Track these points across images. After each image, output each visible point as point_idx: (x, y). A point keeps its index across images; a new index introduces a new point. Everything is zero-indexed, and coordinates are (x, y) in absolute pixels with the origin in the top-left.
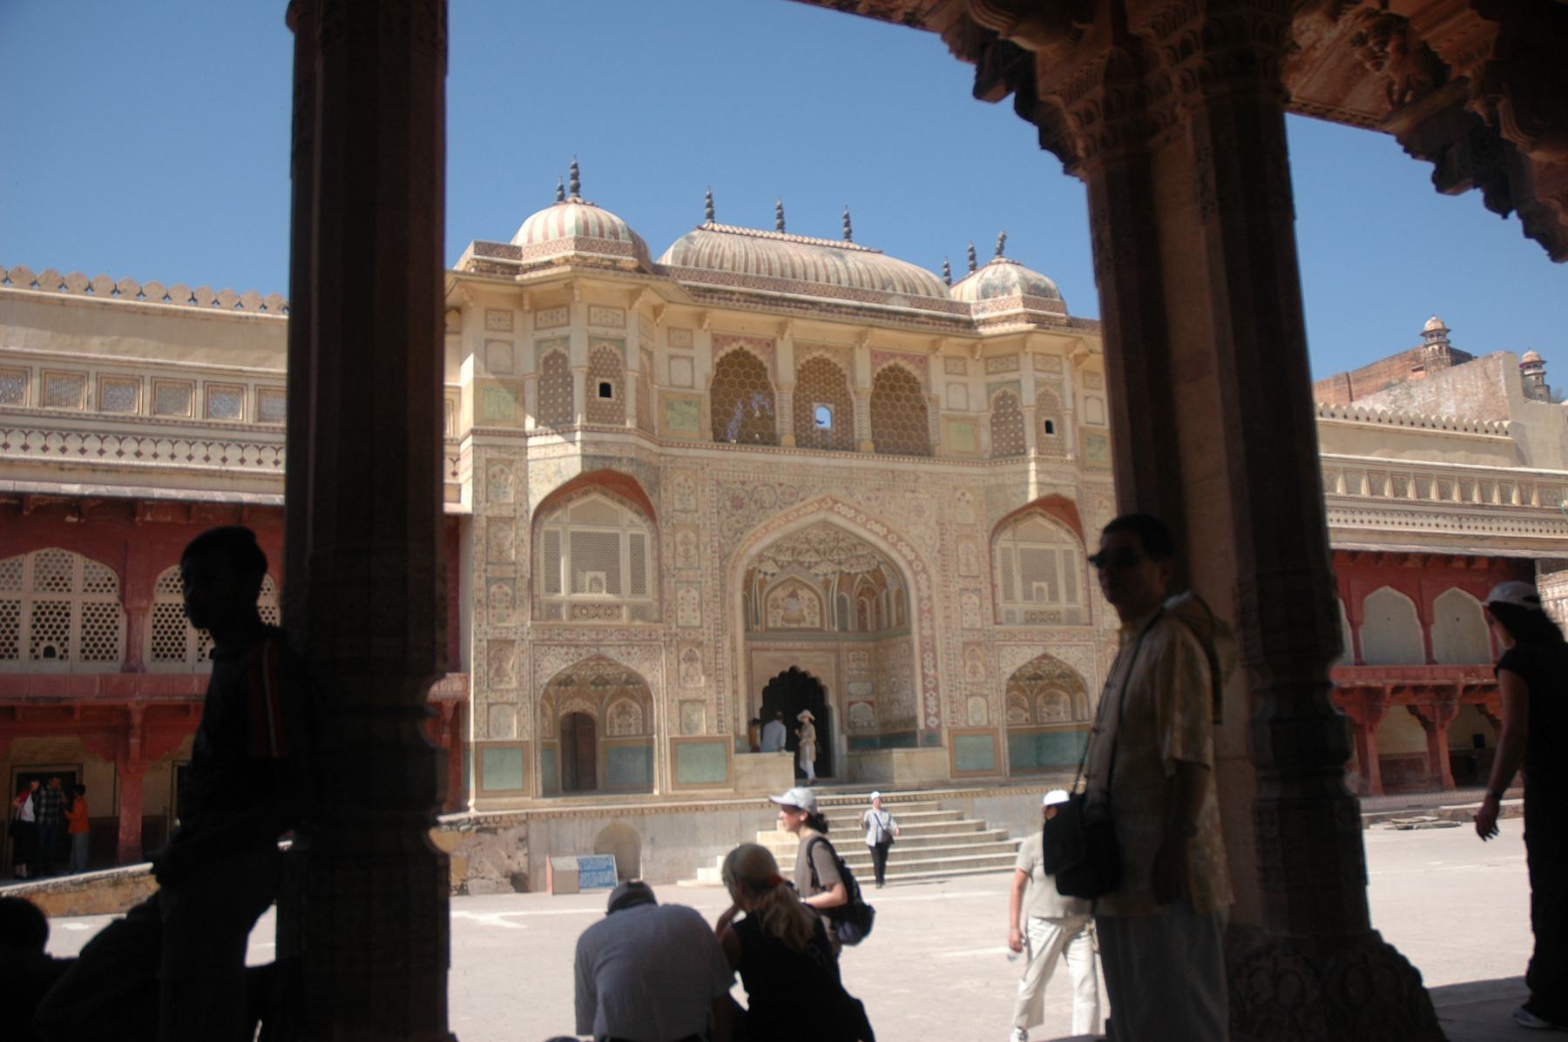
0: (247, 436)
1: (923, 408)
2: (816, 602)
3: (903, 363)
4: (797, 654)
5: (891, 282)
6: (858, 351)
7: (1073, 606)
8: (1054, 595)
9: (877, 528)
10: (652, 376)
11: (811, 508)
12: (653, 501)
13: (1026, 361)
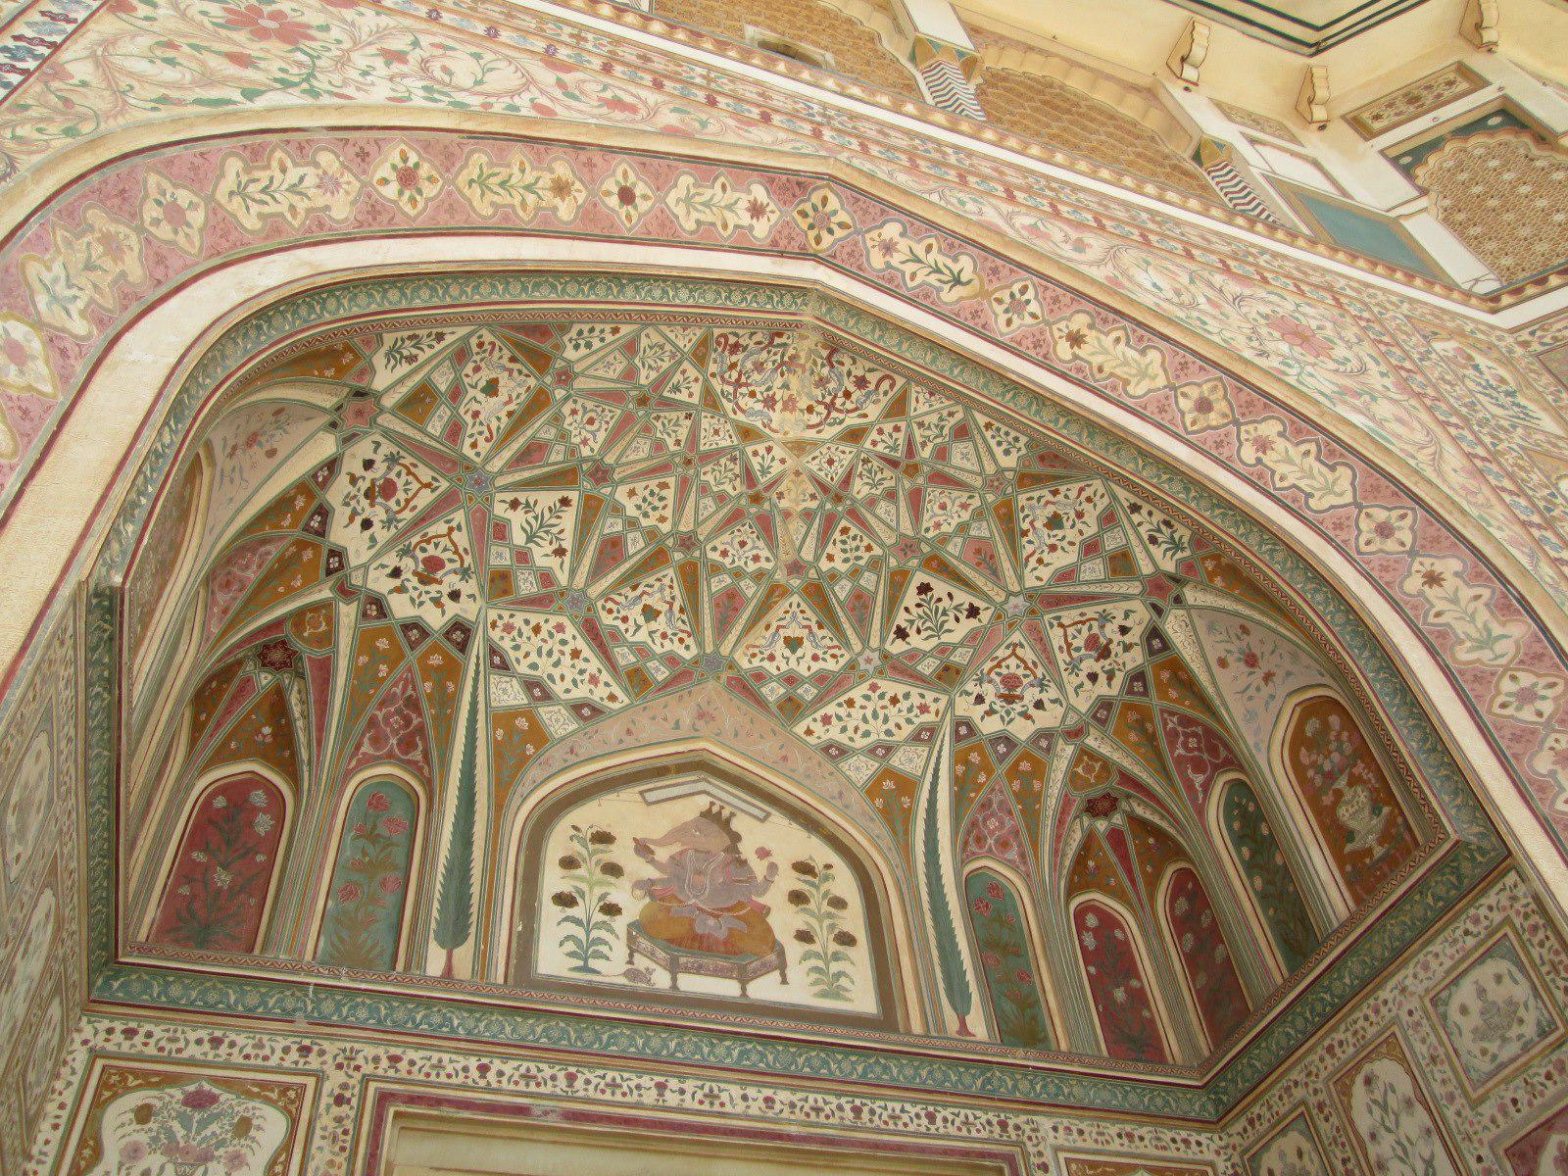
9: (1106, 351)
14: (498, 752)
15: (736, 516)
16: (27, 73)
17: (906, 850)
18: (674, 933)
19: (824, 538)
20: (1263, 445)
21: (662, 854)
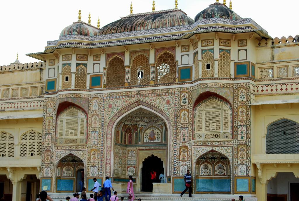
0: (9, 101)
1: (175, 66)
2: (160, 133)
3: (168, 51)
4: (153, 151)
5: (166, 24)
6: (151, 50)
7: (226, 131)
8: (218, 128)
9: (155, 109)
10: (86, 71)
11: (134, 105)
13: (200, 44)
14: (141, 130)
18: (151, 139)
21: (150, 133)
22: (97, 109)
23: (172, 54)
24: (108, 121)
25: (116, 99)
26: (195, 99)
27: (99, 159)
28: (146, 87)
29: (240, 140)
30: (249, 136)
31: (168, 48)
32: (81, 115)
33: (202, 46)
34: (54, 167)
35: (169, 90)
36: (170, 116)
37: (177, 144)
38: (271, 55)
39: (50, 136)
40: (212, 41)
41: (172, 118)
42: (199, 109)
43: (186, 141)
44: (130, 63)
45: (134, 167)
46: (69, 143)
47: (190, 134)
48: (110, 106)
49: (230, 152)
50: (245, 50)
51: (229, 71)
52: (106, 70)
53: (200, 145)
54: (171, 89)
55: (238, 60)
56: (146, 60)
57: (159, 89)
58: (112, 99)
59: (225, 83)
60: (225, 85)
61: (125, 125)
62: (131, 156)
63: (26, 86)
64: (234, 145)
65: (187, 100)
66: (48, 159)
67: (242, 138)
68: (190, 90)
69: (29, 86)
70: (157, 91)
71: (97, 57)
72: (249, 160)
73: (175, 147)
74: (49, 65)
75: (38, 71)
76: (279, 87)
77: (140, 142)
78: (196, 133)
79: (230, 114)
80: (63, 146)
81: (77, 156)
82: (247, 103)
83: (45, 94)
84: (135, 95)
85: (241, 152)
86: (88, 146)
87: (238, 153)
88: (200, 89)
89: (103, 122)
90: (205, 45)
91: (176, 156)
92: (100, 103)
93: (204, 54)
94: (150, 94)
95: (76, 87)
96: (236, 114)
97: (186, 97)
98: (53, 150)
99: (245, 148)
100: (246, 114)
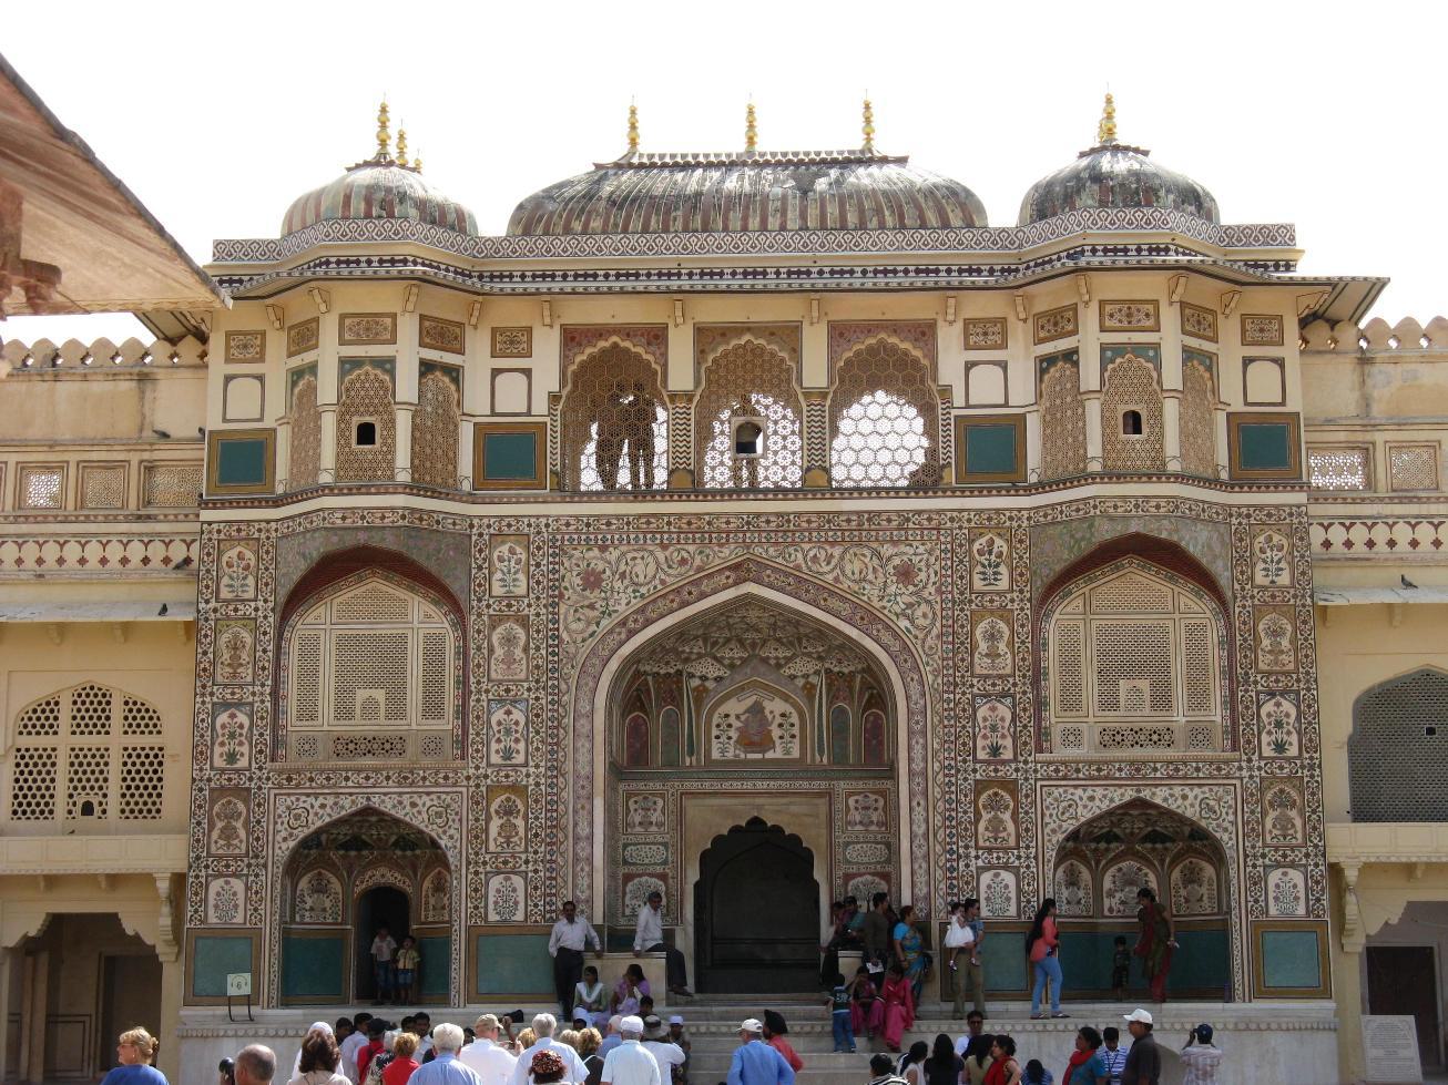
2: (795, 719)
3: (893, 340)
5: (879, 211)
6: (807, 331)
7: (1200, 716)
8: (1162, 700)
9: (834, 603)
12: (455, 587)
13: (1090, 318)
15: (747, 630)
16: (557, 646)
17: (812, 707)
18: (746, 742)
19: (775, 630)
20: (878, 631)
21: (743, 718)
22: (521, 589)
23: (917, 353)
24: (584, 651)
25: (624, 549)
26: (1058, 568)
27: (536, 835)
28: (791, 496)
29: (1273, 759)
30: (1311, 740)
31: (895, 327)
32: (428, 616)
33: (1103, 330)
34: (271, 877)
35: (908, 520)
36: (916, 638)
37: (958, 771)
38: (1356, 394)
39: (242, 718)
40: (1150, 308)
41: (931, 652)
42: (1066, 614)
43: (1003, 757)
44: (697, 383)
45: (663, 877)
46: (354, 753)
47: (1025, 726)
48: (592, 580)
49: (1224, 811)
50: (1274, 360)
51: (1213, 450)
52: (560, 407)
53: (1075, 776)
54: (919, 512)
55: (1247, 404)
56: (776, 372)
57: (859, 513)
58: (603, 549)
59: (1203, 502)
60: (1204, 510)
61: (638, 674)
62: (640, 823)
63: (52, 457)
64: (1241, 779)
65: (1003, 569)
66: (228, 834)
67: (1280, 747)
68: (1015, 524)
69: (73, 458)
70: (849, 521)
71: (512, 342)
72: (1316, 846)
73: (950, 784)
74: (228, 360)
75: (126, 386)
76: (1402, 533)
77: (691, 754)
78: (1053, 720)
79: (1216, 640)
80: (322, 771)
81: (407, 819)
82: (1295, 596)
83: (204, 504)
84: (728, 533)
85: (1277, 813)
86: (472, 771)
87: (1264, 814)
88: (1096, 524)
89: (554, 654)
90: (1118, 325)
91: (960, 824)
92: (538, 565)
93: (1110, 366)
94: (810, 531)
95: (416, 476)
96: (1245, 640)
97: (1000, 555)
98: (260, 788)
99: (1294, 794)
100: (1293, 641)
